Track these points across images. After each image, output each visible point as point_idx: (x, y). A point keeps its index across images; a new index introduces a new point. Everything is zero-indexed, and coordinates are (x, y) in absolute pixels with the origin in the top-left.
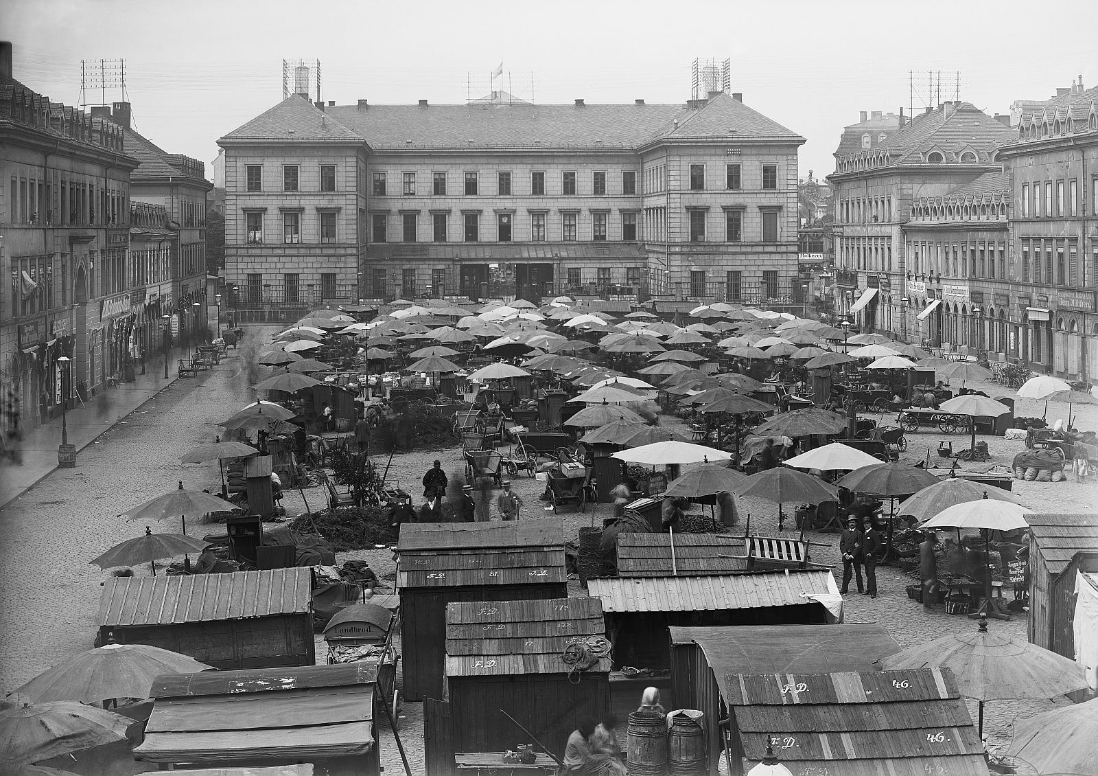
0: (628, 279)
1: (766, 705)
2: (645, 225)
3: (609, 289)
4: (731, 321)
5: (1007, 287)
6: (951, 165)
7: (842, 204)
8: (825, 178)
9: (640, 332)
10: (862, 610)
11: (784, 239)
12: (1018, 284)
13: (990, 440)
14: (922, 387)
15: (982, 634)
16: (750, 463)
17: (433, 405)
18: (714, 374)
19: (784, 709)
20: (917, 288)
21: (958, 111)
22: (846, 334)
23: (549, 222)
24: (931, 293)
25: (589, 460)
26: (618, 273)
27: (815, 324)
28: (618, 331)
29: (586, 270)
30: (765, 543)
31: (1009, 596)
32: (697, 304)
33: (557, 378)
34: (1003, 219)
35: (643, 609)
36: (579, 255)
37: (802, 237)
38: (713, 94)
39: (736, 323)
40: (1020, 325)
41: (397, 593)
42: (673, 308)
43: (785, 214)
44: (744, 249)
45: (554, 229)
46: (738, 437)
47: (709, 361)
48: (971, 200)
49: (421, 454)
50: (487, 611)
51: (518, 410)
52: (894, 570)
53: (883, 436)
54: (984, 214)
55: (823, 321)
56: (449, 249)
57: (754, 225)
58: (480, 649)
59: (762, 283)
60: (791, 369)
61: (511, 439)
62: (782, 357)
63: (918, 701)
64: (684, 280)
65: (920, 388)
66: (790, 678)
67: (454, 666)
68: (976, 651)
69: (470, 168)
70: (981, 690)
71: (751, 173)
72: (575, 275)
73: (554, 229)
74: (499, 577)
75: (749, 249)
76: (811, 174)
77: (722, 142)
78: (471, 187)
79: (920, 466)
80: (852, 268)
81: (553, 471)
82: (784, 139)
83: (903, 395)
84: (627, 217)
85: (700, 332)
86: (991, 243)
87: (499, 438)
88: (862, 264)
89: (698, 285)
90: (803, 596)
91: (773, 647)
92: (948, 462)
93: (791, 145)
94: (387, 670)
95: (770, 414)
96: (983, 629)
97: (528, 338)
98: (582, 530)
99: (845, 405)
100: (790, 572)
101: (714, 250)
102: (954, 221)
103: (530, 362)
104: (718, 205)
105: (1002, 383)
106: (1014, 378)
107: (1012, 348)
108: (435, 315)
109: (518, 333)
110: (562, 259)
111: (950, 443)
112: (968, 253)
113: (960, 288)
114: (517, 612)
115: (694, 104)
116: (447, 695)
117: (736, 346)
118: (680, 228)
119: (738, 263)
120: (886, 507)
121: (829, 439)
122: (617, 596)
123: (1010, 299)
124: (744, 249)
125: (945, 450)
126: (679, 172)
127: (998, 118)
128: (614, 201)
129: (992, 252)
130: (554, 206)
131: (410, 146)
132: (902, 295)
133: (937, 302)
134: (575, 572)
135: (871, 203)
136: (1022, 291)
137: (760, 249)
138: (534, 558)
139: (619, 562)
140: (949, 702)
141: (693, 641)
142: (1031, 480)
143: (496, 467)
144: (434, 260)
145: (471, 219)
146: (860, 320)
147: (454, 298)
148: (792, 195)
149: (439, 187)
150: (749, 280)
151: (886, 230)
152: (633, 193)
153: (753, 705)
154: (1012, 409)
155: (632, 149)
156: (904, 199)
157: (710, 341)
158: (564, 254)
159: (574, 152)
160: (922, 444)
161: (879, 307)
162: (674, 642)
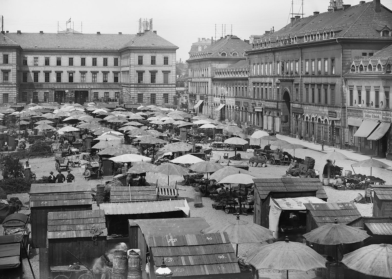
0: (115, 96)
1: (162, 247)
2: (121, 77)
3: (108, 100)
4: (152, 111)
5: (248, 100)
6: (229, 57)
7: (191, 70)
8: (185, 61)
9: (119, 115)
10: (196, 213)
11: (171, 82)
12: (251, 99)
13: (241, 153)
14: (218, 134)
15: (238, 220)
16: (158, 161)
17: (44, 141)
18: (145, 130)
19: (169, 248)
20: (217, 100)
21: (232, 38)
22: (192, 116)
23: (87, 75)
24: (222, 102)
25: (101, 161)
26: (112, 95)
27: (181, 113)
28: (112, 114)
29: (111, 93)
30: (163, 189)
31: (247, 207)
32: (140, 105)
33: (89, 132)
34: (246, 76)
35: (119, 213)
36: (98, 87)
37: (177, 82)
38: (146, 31)
39: (153, 112)
40: (252, 113)
41: (30, 209)
42: (131, 107)
43: (171, 74)
44: (157, 86)
45: (89, 78)
46: (154, 152)
47: (144, 126)
48: (236, 69)
49: (39, 159)
50: (63, 215)
51: (75, 143)
52: (208, 198)
53: (205, 152)
54: (237, 74)
55: (185, 111)
56: (62, 85)
57: (160, 77)
58: (60, 229)
59: (163, 98)
60: (169, 127)
61: (72, 153)
62: (170, 124)
63: (216, 244)
64: (135, 97)
65: (217, 135)
66: (171, 237)
67: (50, 235)
68: (236, 226)
69: (59, 56)
70: (237, 240)
71: (160, 58)
72: (96, 94)
73: (89, 78)
74: (67, 203)
75: (158, 86)
76: (181, 60)
77: (149, 48)
78: (59, 63)
79: (217, 162)
80: (195, 92)
81: (88, 165)
82: (171, 47)
83: (212, 137)
84: (104, 74)
85: (141, 115)
86: (243, 84)
87: (68, 153)
88: (198, 91)
89: (140, 98)
90: (176, 208)
91: (165, 226)
92: (227, 161)
93: (173, 50)
94: (26, 237)
95: (165, 144)
96: (238, 218)
97: (78, 117)
98: (98, 185)
99: (192, 141)
100: (171, 199)
101: (146, 86)
102: (230, 77)
103: (79, 126)
104: (148, 70)
105: (246, 133)
106: (250, 132)
107: (249, 121)
108: (45, 109)
109: (76, 115)
110: (92, 89)
111: (228, 154)
112: (235, 88)
113: (232, 100)
114: (74, 215)
115: (140, 34)
116: (48, 246)
117: (154, 120)
118: (134, 79)
119: (155, 91)
120: (205, 176)
121: (186, 153)
122: (110, 209)
123: (249, 104)
124: (157, 86)
125: (226, 156)
126: (134, 57)
127: (245, 41)
128: (111, 68)
129: (243, 88)
130: (89, 70)
131: (37, 48)
132: (212, 102)
133: (224, 105)
134: (95, 200)
135: (201, 70)
136: (253, 101)
137: (162, 86)
138: (80, 196)
139: (111, 197)
140: (226, 244)
141: (137, 224)
142: (255, 167)
143: (67, 163)
144: (45, 89)
145: (59, 74)
146: (197, 111)
147: (52, 102)
148: (174, 67)
149: (47, 63)
150: (158, 97)
151: (206, 80)
152: (117, 65)
153: (158, 247)
154: (249, 142)
155: (117, 50)
156: (213, 69)
157: (144, 118)
158: (92, 87)
159: (96, 51)
160: (217, 155)
161: (204, 107)
162: (130, 225)
